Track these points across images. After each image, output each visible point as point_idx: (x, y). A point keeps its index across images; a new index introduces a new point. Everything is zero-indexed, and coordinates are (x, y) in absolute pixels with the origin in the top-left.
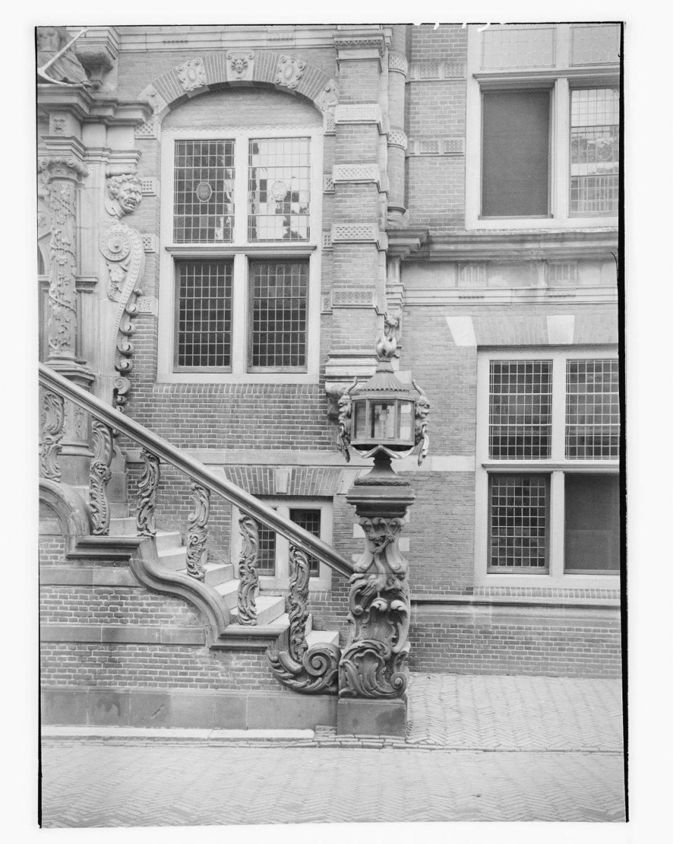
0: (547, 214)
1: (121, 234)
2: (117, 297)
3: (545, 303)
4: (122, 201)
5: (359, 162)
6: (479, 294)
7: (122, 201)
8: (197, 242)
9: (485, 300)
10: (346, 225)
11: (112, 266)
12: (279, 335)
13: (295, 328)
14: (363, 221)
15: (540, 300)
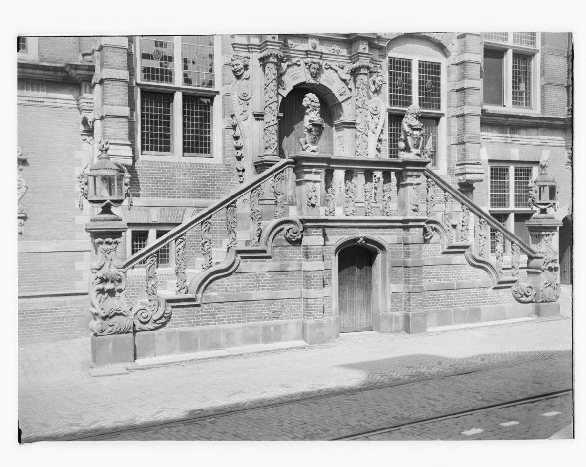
0: (501, 104)
1: (377, 101)
2: (376, 131)
3: (510, 143)
4: (376, 86)
5: (474, 80)
6: (42, 100)
7: (376, 86)
8: (430, 109)
9: (45, 104)
10: (470, 107)
11: (373, 116)
12: (152, 134)
13: (165, 131)
14: (475, 105)
15: (509, 142)
